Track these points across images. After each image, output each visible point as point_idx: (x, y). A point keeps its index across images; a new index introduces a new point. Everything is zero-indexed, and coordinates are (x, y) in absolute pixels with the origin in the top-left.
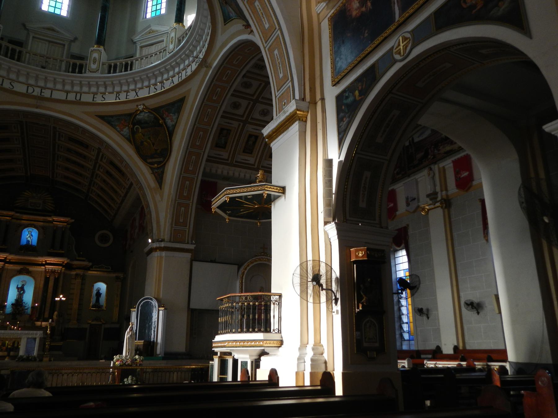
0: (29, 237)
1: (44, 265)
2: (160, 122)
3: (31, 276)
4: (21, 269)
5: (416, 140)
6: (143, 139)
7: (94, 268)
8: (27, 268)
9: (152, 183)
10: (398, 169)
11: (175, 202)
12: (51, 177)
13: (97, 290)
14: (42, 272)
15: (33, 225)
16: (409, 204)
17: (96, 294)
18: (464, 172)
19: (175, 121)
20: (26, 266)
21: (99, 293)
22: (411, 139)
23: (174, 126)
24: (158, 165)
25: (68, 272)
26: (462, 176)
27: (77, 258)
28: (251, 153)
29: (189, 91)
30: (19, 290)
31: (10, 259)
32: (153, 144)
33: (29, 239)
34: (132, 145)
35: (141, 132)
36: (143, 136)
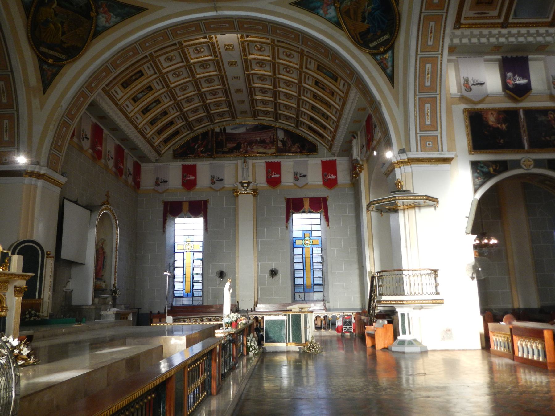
2: (93, 14)
5: (228, 131)
6: (51, 18)
9: (34, 79)
10: (202, 148)
11: (62, 118)
16: (215, 183)
18: (275, 174)
19: (112, 24)
22: (222, 128)
23: (106, 29)
24: (54, 61)
26: (274, 176)
28: (125, 88)
29: (160, 8)
32: (63, 33)
34: (28, 17)
35: (53, 9)
36: (53, 15)
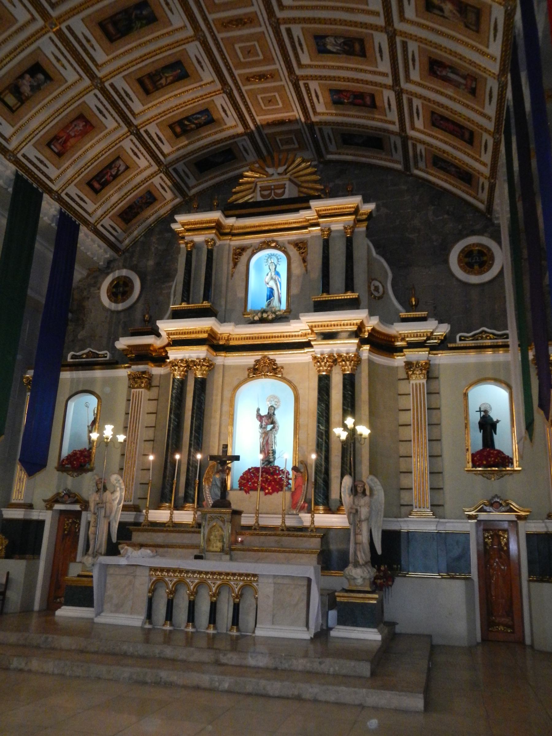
0: (272, 278)
1: (308, 345)
3: (283, 379)
4: (257, 361)
7: (460, 340)
8: (271, 357)
12: (303, 120)
13: (480, 411)
14: (309, 363)
15: (274, 241)
17: (480, 423)
20: (266, 353)
21: (491, 419)
25: (381, 360)
27: (403, 314)
30: (264, 423)
31: (228, 339)
33: (272, 284)
